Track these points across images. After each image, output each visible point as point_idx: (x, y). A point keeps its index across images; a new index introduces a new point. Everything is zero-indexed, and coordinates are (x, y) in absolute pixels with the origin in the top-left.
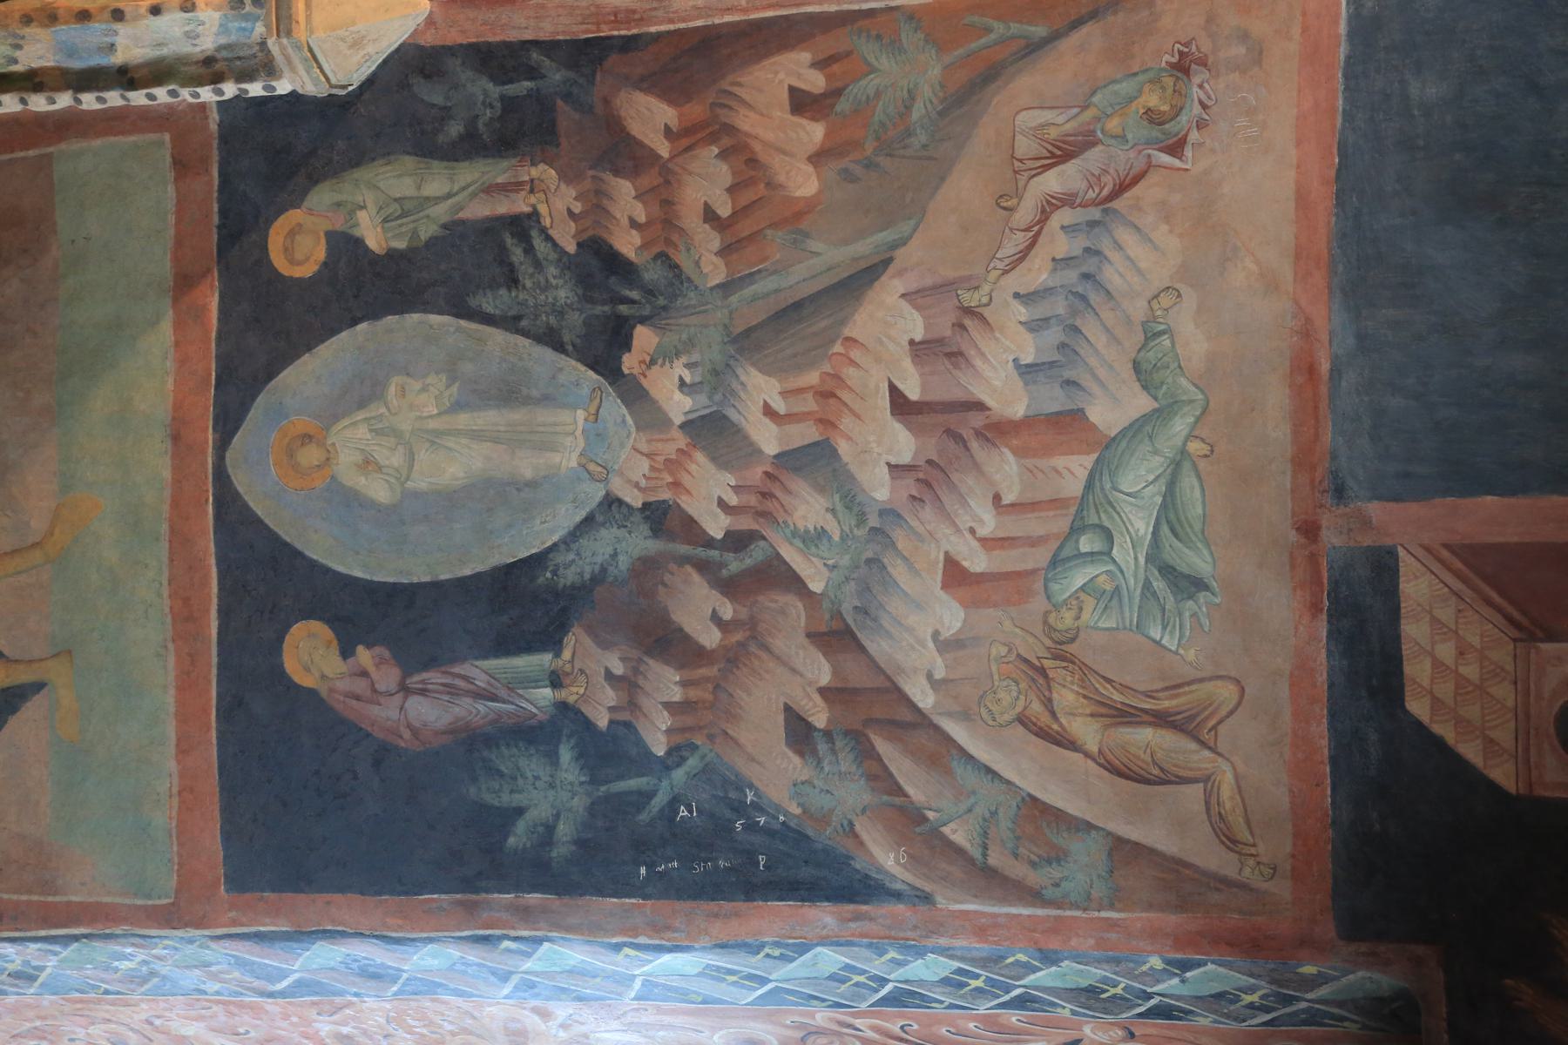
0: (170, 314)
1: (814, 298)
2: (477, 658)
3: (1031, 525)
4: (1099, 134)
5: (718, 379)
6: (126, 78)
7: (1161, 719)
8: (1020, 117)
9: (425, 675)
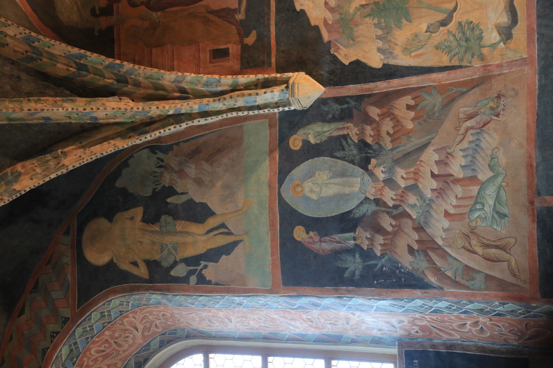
0: (268, 158)
1: (412, 151)
2: (337, 234)
3: (465, 202)
4: (479, 112)
5: (390, 170)
6: (259, 107)
7: (497, 247)
8: (460, 109)
9: (325, 238)
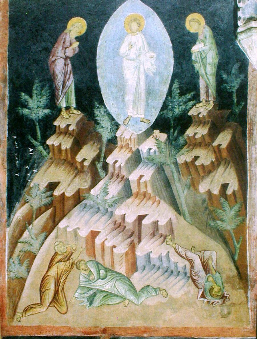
1: (171, 191)
2: (75, 82)
4: (209, 275)
5: (151, 160)
7: (56, 292)
8: (215, 252)
9: (70, 65)
